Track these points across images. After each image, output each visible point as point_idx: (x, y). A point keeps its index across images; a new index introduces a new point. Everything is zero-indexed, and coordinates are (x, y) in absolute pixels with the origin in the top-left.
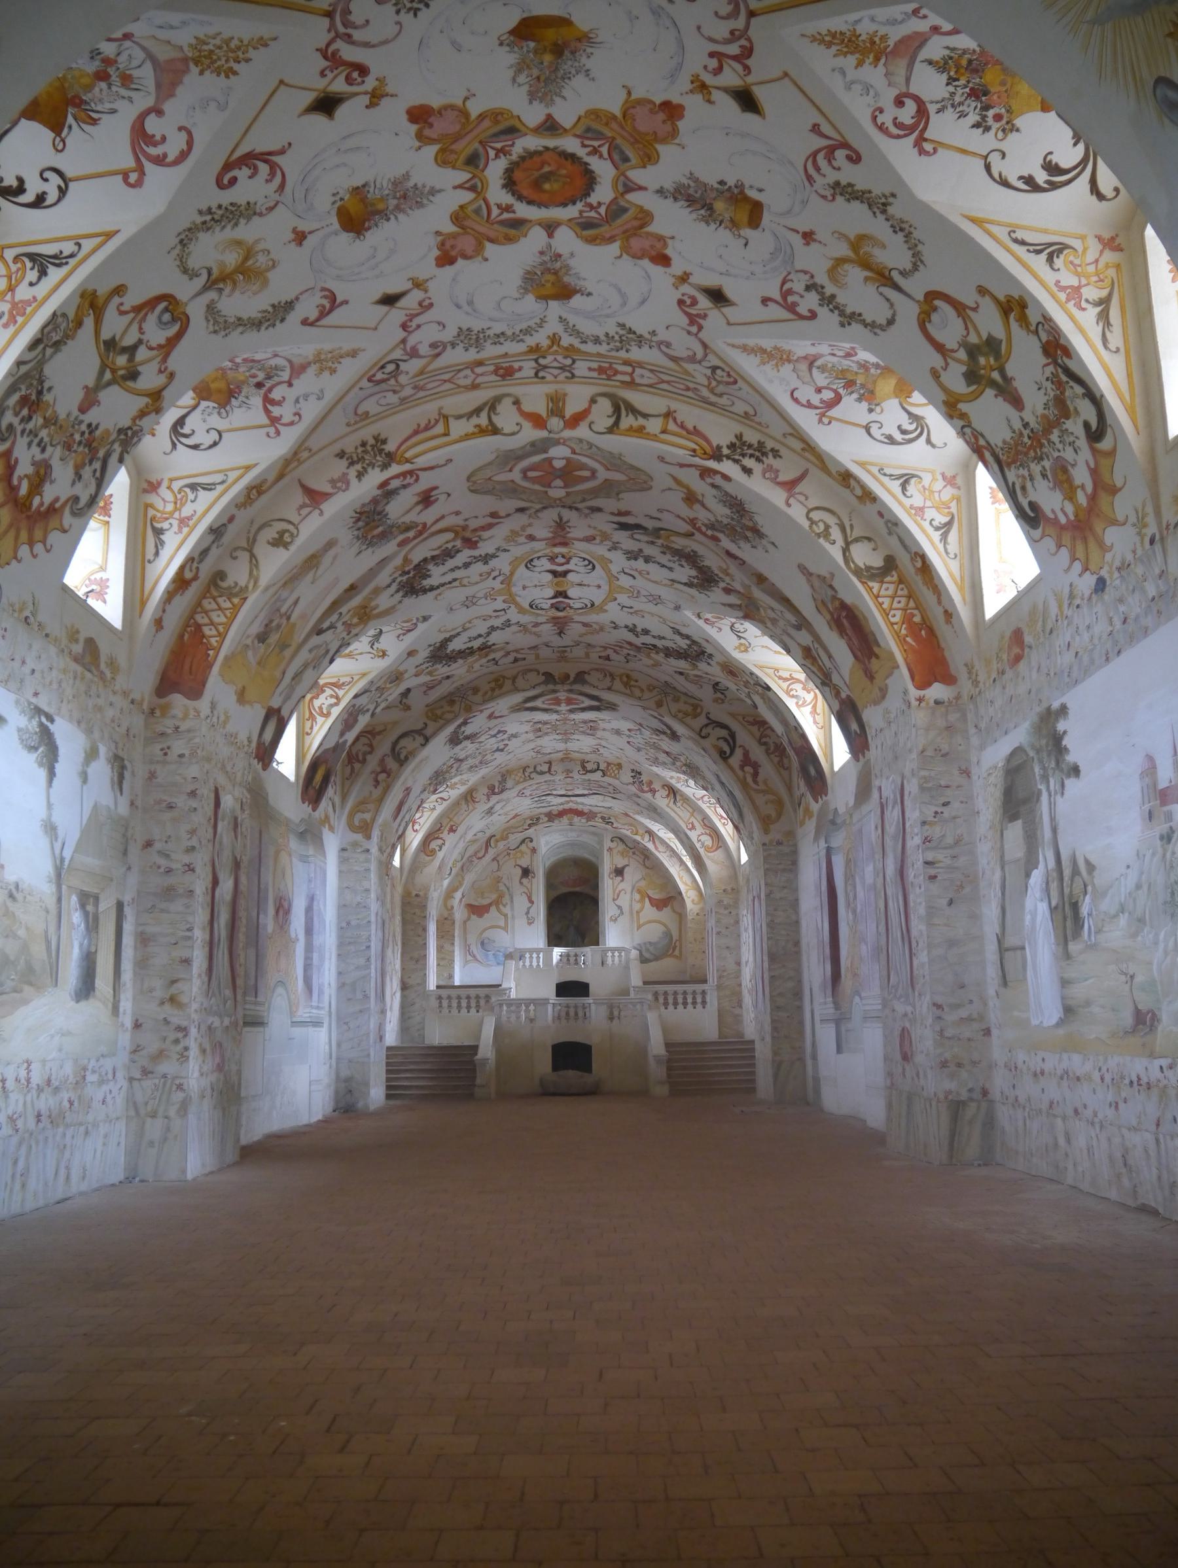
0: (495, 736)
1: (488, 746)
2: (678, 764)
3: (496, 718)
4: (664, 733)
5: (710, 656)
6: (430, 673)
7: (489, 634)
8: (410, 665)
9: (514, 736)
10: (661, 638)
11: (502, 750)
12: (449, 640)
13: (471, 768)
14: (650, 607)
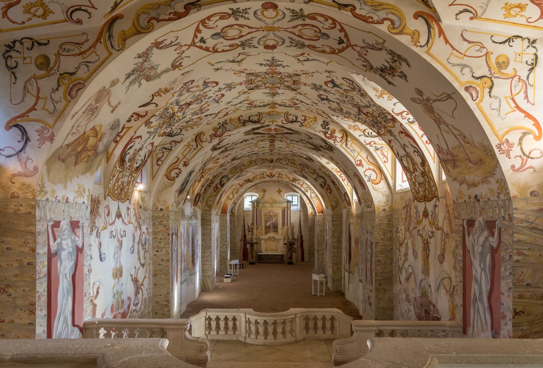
0: (327, 99)
1: (337, 96)
2: (176, 108)
4: (218, 144)
9: (316, 87)
11: (332, 82)
13: (363, 94)
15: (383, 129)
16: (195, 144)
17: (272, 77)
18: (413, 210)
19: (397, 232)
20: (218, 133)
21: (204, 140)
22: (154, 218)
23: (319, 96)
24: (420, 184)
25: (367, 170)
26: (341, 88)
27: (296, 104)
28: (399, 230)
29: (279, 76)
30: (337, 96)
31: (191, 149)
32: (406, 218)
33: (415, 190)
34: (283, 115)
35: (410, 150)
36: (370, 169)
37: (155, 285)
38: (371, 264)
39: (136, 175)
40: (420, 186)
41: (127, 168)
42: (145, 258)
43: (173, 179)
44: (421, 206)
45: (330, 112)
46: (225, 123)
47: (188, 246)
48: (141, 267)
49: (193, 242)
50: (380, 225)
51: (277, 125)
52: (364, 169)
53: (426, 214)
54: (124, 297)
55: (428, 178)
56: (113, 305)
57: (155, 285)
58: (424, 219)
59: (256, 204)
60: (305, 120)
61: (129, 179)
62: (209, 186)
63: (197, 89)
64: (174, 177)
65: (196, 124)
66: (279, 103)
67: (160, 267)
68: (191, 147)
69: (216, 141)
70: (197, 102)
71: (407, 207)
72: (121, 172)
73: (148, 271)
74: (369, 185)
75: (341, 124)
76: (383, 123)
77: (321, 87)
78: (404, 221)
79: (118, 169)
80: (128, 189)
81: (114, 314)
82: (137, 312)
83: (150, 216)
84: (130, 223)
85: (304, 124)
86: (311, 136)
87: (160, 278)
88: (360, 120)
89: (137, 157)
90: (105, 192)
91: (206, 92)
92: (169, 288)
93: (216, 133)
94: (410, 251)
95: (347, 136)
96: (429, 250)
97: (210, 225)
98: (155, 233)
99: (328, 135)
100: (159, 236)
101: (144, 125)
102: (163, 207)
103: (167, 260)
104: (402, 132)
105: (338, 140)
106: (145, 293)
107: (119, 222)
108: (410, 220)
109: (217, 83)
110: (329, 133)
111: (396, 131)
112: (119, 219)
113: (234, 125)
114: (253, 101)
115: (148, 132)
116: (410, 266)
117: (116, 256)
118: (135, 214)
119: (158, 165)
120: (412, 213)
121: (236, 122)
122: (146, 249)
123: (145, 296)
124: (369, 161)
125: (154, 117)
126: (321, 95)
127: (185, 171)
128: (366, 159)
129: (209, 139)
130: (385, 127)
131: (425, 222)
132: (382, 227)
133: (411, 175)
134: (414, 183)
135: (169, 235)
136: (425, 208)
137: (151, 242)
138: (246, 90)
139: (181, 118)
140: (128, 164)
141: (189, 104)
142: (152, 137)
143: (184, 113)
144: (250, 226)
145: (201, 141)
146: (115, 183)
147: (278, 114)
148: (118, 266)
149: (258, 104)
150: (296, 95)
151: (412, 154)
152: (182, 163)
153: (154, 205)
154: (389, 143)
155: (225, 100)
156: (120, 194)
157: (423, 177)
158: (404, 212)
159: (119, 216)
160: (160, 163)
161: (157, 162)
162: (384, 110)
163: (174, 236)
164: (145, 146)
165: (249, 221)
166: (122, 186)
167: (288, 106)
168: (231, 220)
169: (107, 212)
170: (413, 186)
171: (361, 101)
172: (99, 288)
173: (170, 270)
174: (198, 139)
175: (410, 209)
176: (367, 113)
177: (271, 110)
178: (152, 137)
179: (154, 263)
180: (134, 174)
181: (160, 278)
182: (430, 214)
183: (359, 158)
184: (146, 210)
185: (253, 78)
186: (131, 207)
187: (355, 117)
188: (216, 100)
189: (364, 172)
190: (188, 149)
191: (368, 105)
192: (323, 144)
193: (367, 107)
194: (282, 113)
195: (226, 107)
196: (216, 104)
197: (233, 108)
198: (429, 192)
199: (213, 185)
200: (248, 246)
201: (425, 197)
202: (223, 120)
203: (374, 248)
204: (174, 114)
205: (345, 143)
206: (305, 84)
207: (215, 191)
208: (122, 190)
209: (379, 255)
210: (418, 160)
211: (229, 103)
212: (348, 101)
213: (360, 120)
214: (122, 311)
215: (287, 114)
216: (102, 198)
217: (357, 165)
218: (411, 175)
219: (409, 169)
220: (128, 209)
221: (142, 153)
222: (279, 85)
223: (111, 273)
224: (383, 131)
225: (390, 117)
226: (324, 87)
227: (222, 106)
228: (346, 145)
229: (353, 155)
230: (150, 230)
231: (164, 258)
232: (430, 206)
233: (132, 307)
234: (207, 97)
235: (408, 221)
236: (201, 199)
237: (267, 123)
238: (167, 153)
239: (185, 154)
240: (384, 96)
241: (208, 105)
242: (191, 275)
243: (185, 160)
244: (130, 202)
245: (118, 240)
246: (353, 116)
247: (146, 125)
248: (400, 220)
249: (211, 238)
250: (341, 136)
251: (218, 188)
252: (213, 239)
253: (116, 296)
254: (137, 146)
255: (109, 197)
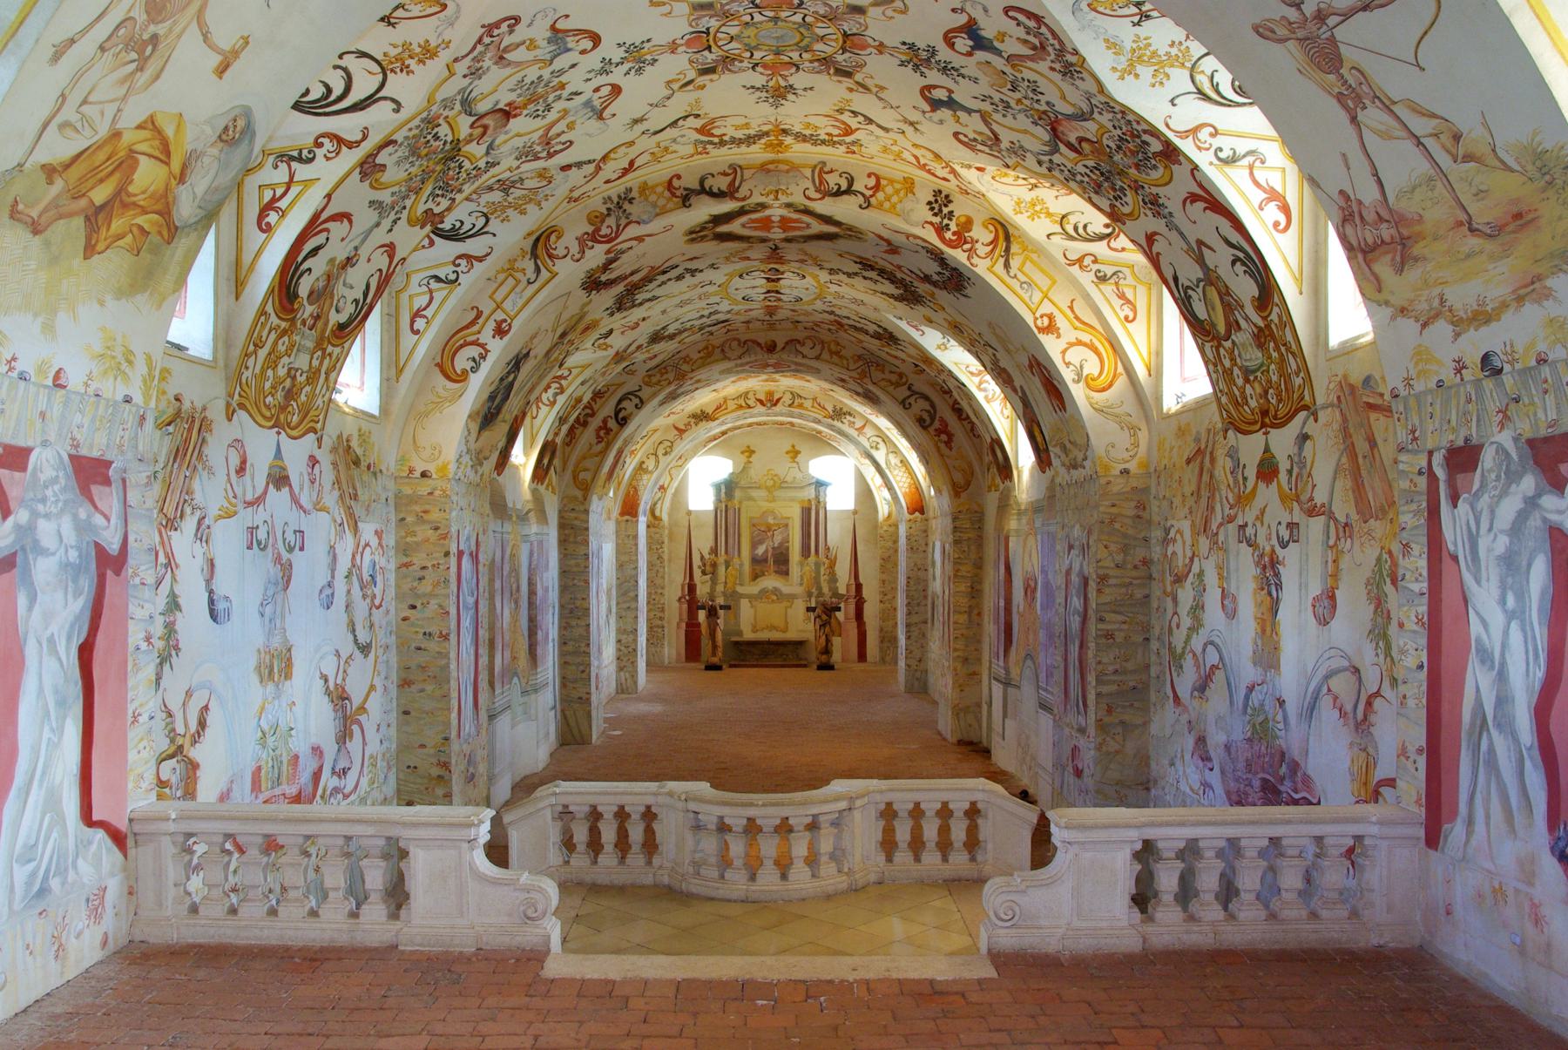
0: (951, 104)
1: (984, 87)
2: (464, 125)
3: (889, 242)
4: (606, 267)
5: (612, 314)
6: (933, 295)
7: (856, 274)
8: (939, 317)
9: (917, 58)
10: (664, 283)
11: (971, 29)
12: (892, 296)
13: (1072, 66)
14: (685, 297)
15: (1129, 197)
16: (529, 266)
17: (776, 19)
18: (1223, 464)
19: (1166, 541)
20: (605, 231)
21: (561, 251)
22: (401, 502)
23: (925, 91)
24: (1247, 372)
25: (1071, 345)
26: (998, 53)
27: (848, 131)
28: (1172, 534)
29: (798, 18)
30: (984, 87)
31: (518, 282)
32: (1197, 493)
33: (1230, 395)
34: (808, 173)
35: (1220, 258)
36: (1079, 343)
37: (406, 713)
38: (1081, 646)
39: (337, 350)
40: (1247, 381)
41: (304, 323)
42: (372, 626)
43: (461, 378)
44: (1251, 447)
45: (958, 155)
46: (626, 198)
47: (516, 602)
48: (357, 652)
49: (532, 592)
50: (1112, 521)
51: (788, 205)
52: (1061, 344)
53: (1267, 470)
54: (300, 745)
55: (1277, 348)
56: (259, 769)
57: (406, 713)
58: (1262, 485)
59: (727, 490)
60: (877, 187)
61: (315, 363)
62: (582, 423)
63: (530, 56)
64: (465, 372)
65: (533, 197)
66: (797, 128)
67: (421, 658)
68: (519, 275)
69: (596, 255)
70: (532, 107)
71: (1201, 456)
72: (284, 332)
73: (382, 667)
74: (1078, 392)
75: (991, 195)
76: (1133, 171)
77: (933, 51)
78: (1191, 501)
79: (274, 320)
80: (312, 397)
81: (262, 797)
82: (346, 797)
83: (391, 495)
84: (319, 507)
85: (873, 200)
86: (899, 240)
87: (422, 690)
88: (1056, 173)
89: (340, 290)
90: (231, 396)
91: (562, 72)
92: (448, 724)
93: (598, 230)
94: (1213, 598)
95: (1007, 238)
96: (1279, 586)
97: (586, 542)
98: (404, 549)
99: (948, 235)
100: (419, 559)
101: (356, 175)
102: (431, 468)
103: (441, 635)
104: (1194, 198)
105: (982, 250)
106: (373, 737)
107: (278, 499)
108: (1211, 498)
109: (596, 39)
110: (953, 227)
111: (1173, 196)
112: (278, 489)
113: (654, 205)
114: (713, 121)
115: (372, 203)
116: (1212, 643)
117: (268, 610)
118: (338, 481)
119: (417, 332)
120: (1219, 473)
121: (661, 195)
122: (374, 596)
123: (374, 747)
124: (1077, 318)
125: (390, 149)
126: (930, 88)
127: (499, 350)
128: (1069, 312)
129: (575, 248)
130: (1137, 187)
131: (1267, 495)
132: (1117, 526)
133: (1217, 349)
134: (1228, 373)
135: (447, 554)
136: (1267, 450)
137: (392, 577)
138: (691, 74)
139: (482, 164)
140: (310, 309)
141: (507, 114)
142: (386, 223)
143: (491, 147)
144: (707, 556)
145: (550, 256)
146: (263, 371)
147: (794, 168)
148: (276, 642)
149: (731, 132)
150: (848, 96)
151: (1224, 270)
152: (491, 325)
153: (402, 460)
154: (1148, 244)
155: (624, 108)
156: (283, 408)
157: (1261, 346)
158: (1190, 474)
159: (280, 479)
160: (420, 324)
161: (412, 322)
162: (1140, 119)
163: (466, 561)
164: (364, 253)
165: (703, 543)
166: (288, 383)
167: (823, 142)
168: (649, 537)
169: (235, 461)
170: (1222, 385)
171: (1063, 97)
172: (206, 708)
173: (453, 666)
174: (541, 251)
175: (1213, 460)
176: (1081, 140)
177: (770, 156)
178: (386, 223)
179: (402, 645)
180: (330, 349)
181: (422, 690)
182: (1284, 466)
183: (1047, 308)
184: (375, 474)
185: (714, 23)
186: (325, 457)
187: (1040, 163)
188: (593, 109)
189: (1064, 352)
190: (511, 281)
191: (1085, 107)
192: (932, 268)
193: (1082, 117)
194: (805, 166)
195: (629, 136)
196: (594, 124)
197: (648, 143)
198: (1279, 395)
199: (595, 422)
200: (702, 615)
201: (1265, 413)
202: (622, 189)
203: (1092, 594)
204: (456, 145)
205: (1002, 260)
206: (881, 48)
207: (599, 439)
208: (290, 395)
209: (1108, 616)
210: (1245, 289)
211: (636, 121)
212: (1019, 101)
213: (1056, 173)
214: (292, 790)
215: (821, 170)
216: (217, 412)
217: (1041, 330)
218: (1217, 349)
219: (1213, 325)
220: (313, 461)
221: (358, 277)
222: (795, 56)
223: (253, 663)
224: (1130, 201)
225: (1156, 146)
226: (944, 53)
227: (614, 132)
228: (1007, 265)
229: (1026, 296)
230: (390, 539)
231: (434, 629)
232: (1282, 441)
233: (328, 781)
234: (565, 94)
235: (1204, 502)
236: (556, 462)
237: (757, 199)
238: (445, 293)
239: (499, 296)
240: (1139, 69)
241: (571, 127)
242: (524, 693)
243: (499, 316)
244: (319, 440)
245: (278, 559)
246: (1031, 161)
247: (364, 175)
248: (1177, 501)
249: (587, 582)
250: (991, 237)
251: (608, 431)
252: (593, 586)
253: (270, 741)
254: (337, 250)
255: (242, 415)
